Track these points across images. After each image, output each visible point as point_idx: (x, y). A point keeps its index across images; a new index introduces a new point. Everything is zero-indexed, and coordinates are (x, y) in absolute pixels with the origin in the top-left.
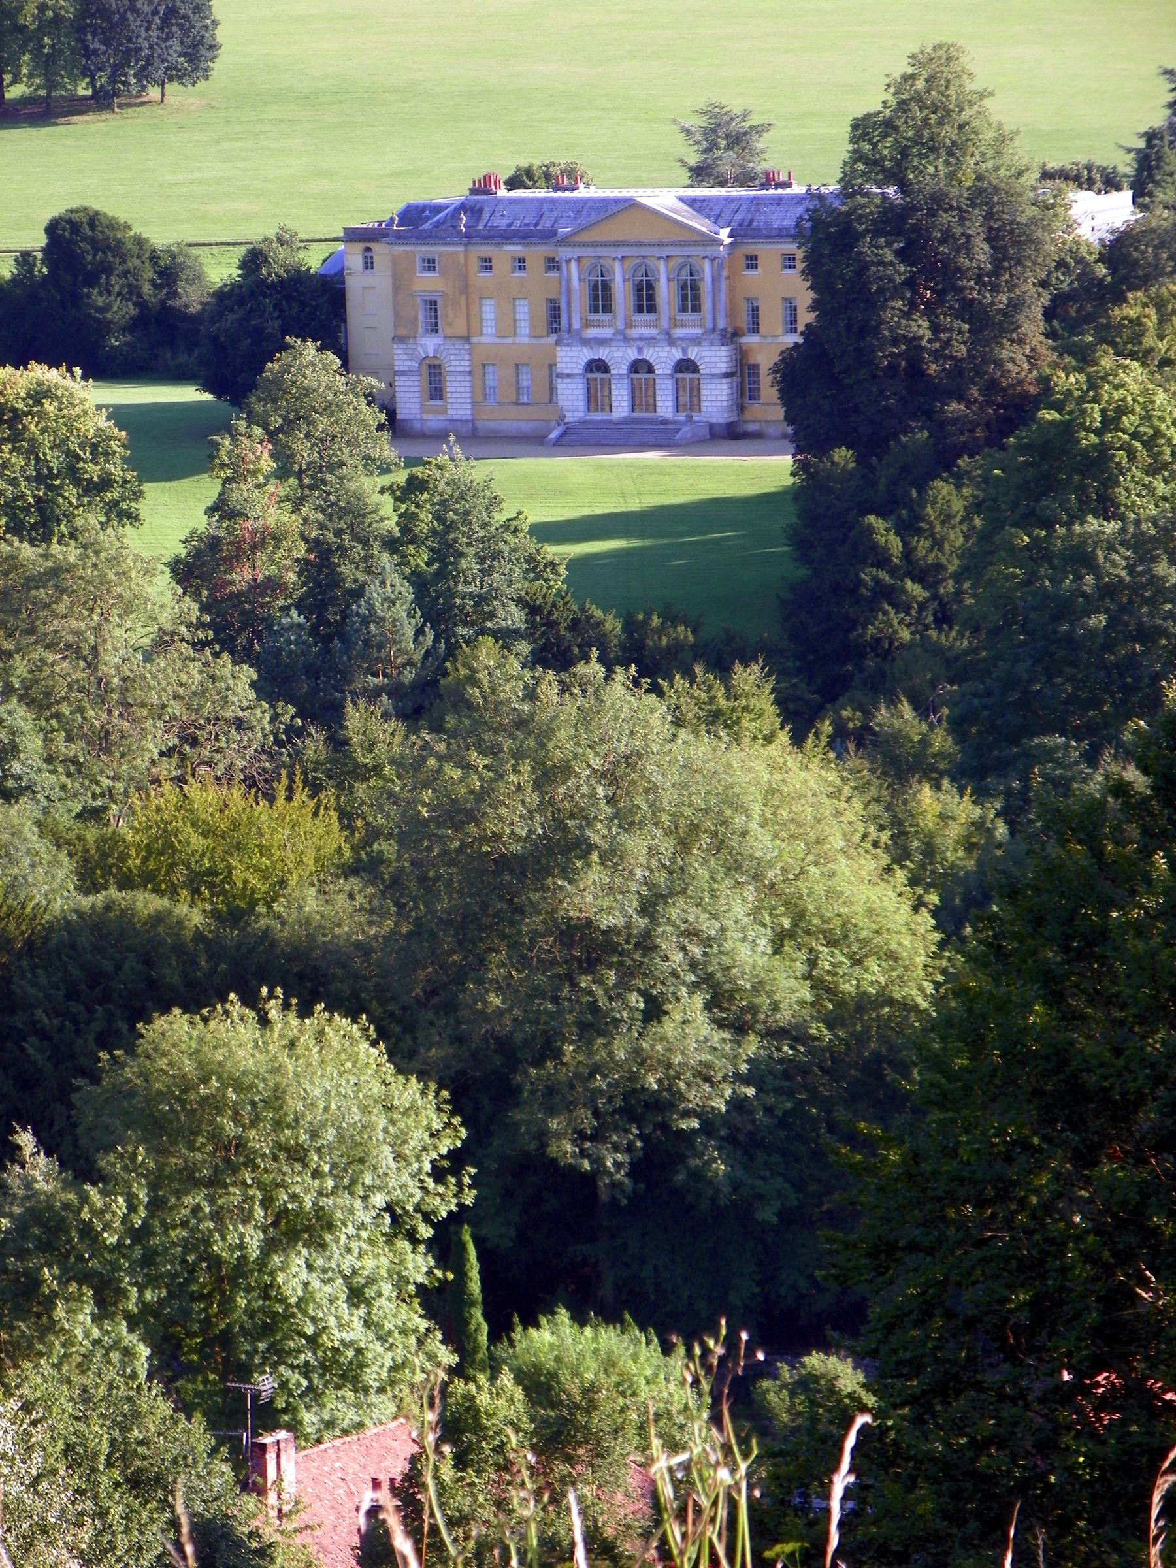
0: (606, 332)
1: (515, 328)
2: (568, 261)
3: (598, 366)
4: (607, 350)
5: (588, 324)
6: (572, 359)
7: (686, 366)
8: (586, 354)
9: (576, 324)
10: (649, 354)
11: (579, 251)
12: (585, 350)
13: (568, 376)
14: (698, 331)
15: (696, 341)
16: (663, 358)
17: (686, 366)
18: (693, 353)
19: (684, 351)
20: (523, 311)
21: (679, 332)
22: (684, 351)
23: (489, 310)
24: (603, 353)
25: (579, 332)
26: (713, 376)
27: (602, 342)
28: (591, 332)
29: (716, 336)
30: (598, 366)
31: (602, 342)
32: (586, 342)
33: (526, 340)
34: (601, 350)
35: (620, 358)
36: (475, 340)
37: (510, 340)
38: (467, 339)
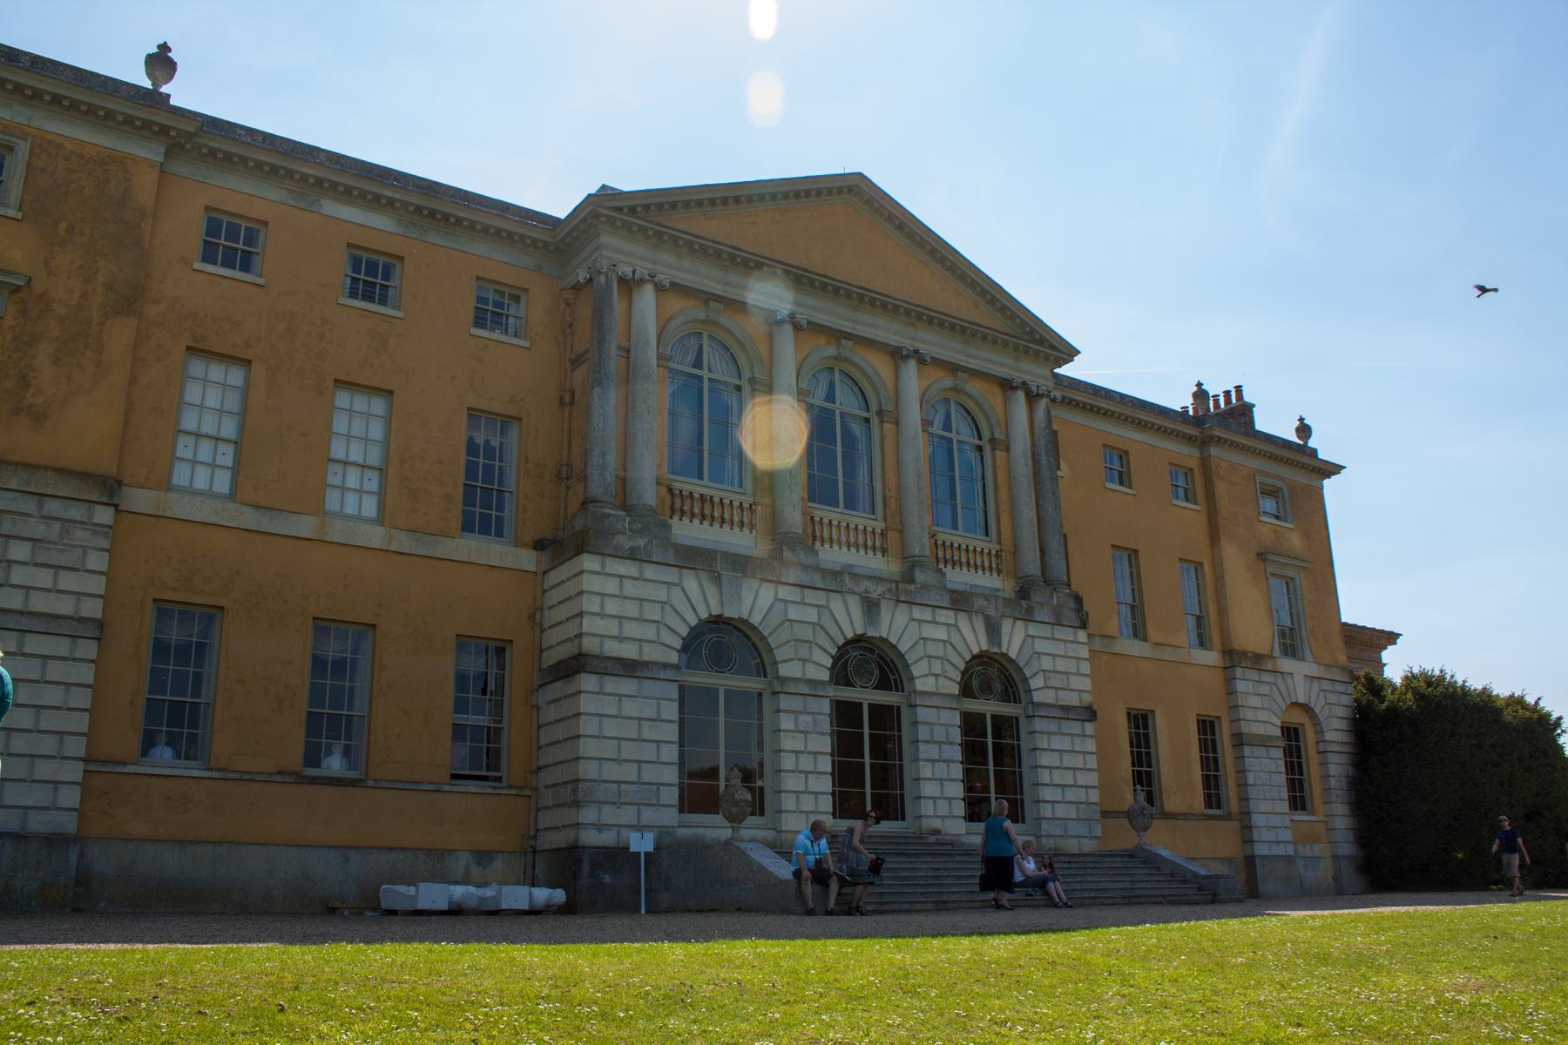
2: (629, 285)
5: (678, 505)
8: (697, 598)
11: (671, 266)
12: (691, 583)
13: (629, 668)
16: (934, 644)
19: (993, 630)
20: (357, 430)
22: (993, 630)
23: (210, 398)
30: (723, 641)
32: (693, 558)
36: (140, 499)
38: (109, 487)
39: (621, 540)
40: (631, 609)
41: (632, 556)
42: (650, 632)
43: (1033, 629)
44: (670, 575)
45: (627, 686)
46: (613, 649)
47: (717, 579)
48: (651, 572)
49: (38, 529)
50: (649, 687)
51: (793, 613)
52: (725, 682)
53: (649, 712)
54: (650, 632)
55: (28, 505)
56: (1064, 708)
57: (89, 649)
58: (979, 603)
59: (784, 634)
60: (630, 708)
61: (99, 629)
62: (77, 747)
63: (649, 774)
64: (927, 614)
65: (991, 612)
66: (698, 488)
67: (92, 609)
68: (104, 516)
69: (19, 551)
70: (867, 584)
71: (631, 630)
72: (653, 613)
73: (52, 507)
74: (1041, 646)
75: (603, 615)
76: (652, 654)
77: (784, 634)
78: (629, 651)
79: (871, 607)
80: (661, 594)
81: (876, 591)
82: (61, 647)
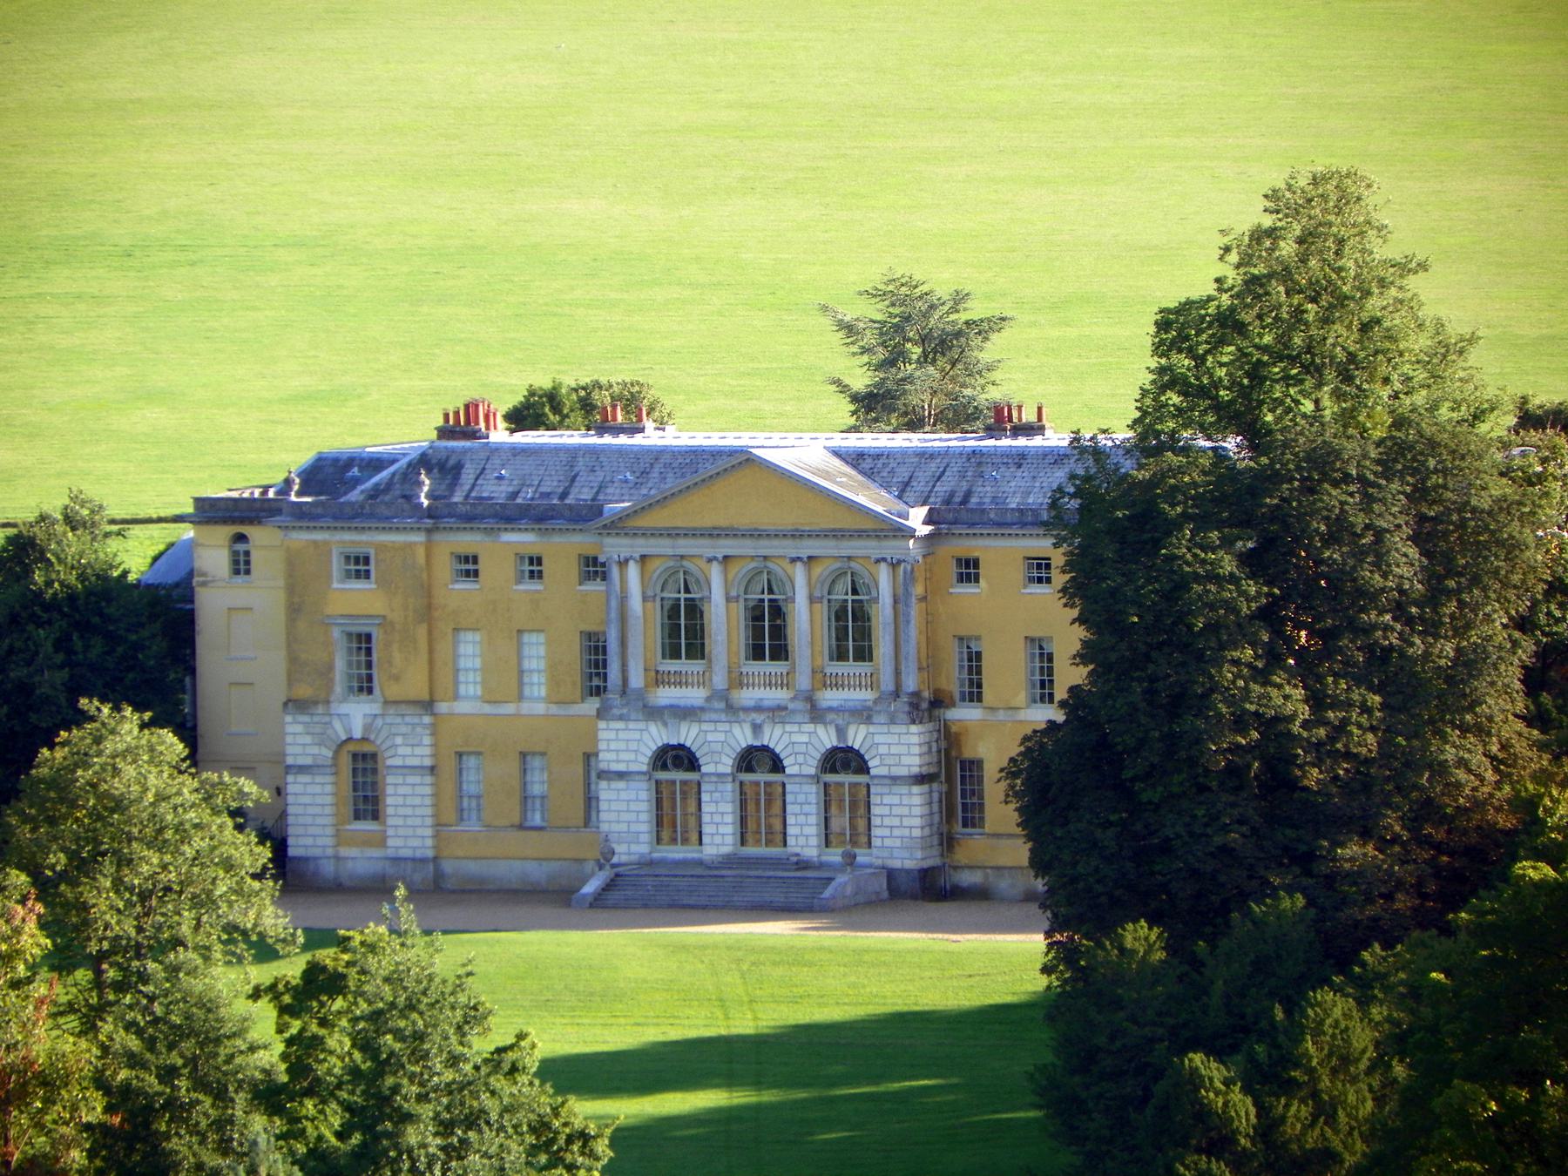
1: (521, 684)
4: (695, 729)
5: (659, 679)
7: (843, 760)
9: (637, 680)
12: (653, 728)
13: (621, 775)
14: (867, 695)
17: (843, 760)
18: (857, 737)
22: (841, 732)
23: (470, 651)
24: (687, 734)
26: (895, 780)
28: (666, 695)
29: (902, 705)
32: (654, 713)
33: (540, 708)
34: (684, 727)
36: (442, 707)
37: (510, 709)
38: (428, 705)
40: (622, 746)
44: (642, 725)
45: (621, 784)
54: (632, 756)
57: (428, 779)
60: (624, 795)
61: (432, 769)
62: (429, 821)
67: (428, 762)
68: (427, 719)
69: (399, 740)
72: (633, 746)
80: (637, 735)
82: (417, 779)
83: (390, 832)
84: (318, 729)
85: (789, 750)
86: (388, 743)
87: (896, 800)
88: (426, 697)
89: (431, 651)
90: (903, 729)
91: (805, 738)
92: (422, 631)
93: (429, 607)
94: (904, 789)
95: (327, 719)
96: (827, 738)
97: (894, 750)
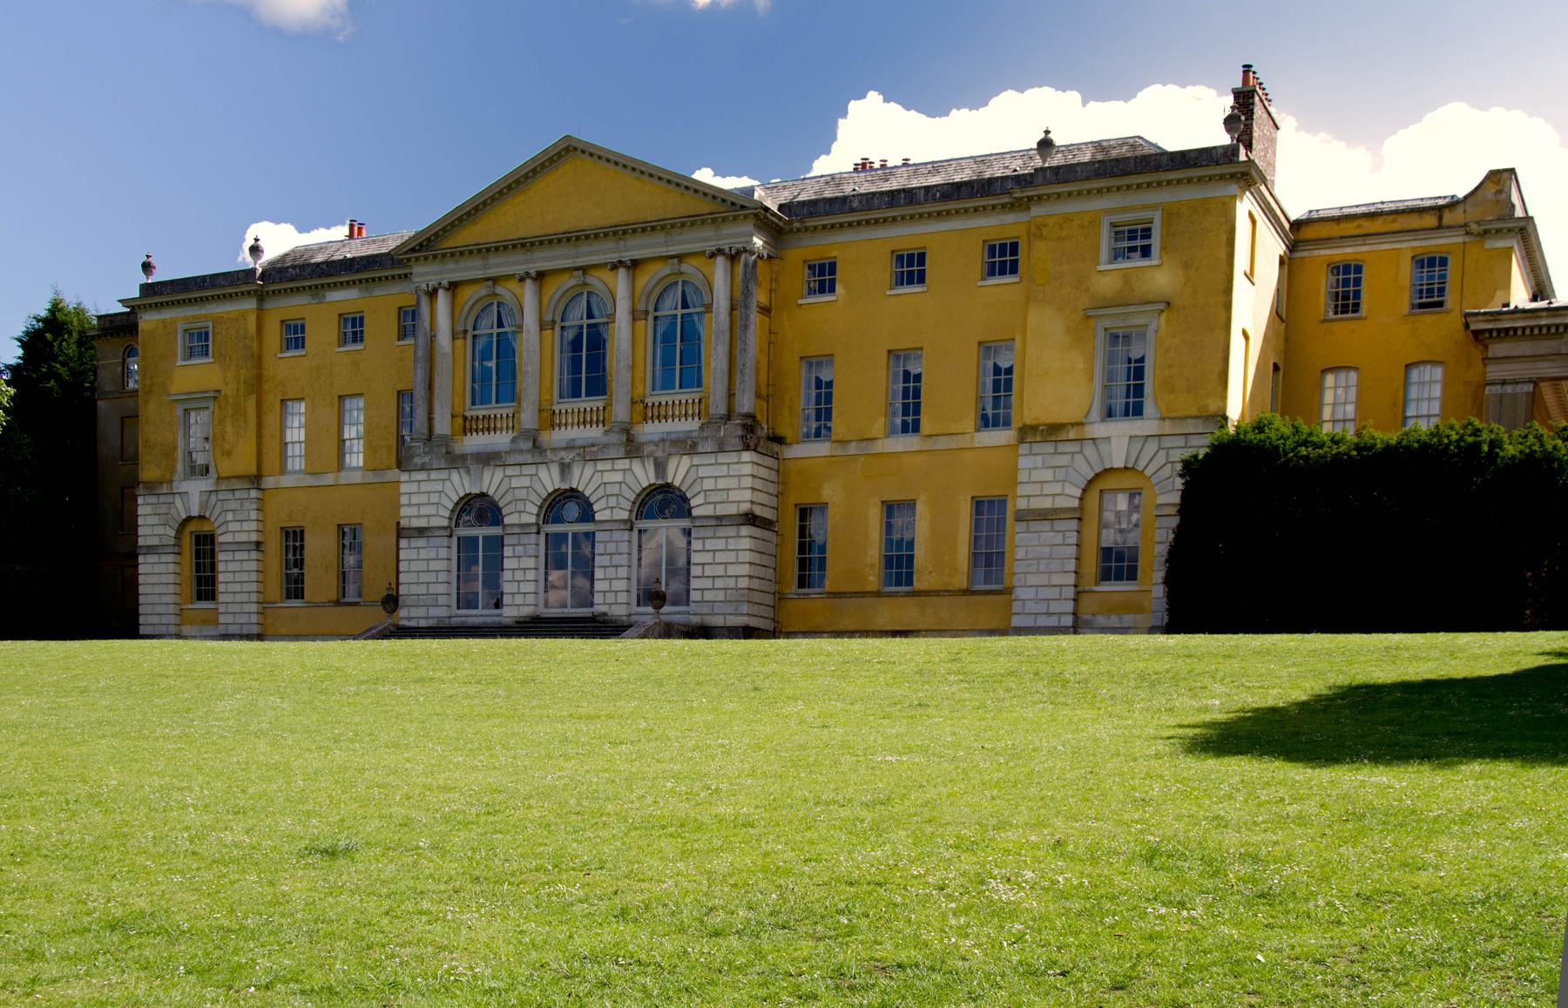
0: (500, 440)
2: (432, 294)
3: (479, 508)
5: (468, 426)
6: (428, 496)
7: (663, 501)
8: (459, 484)
9: (442, 427)
10: (584, 478)
12: (455, 476)
13: (421, 532)
14: (692, 425)
15: (687, 446)
17: (663, 501)
18: (678, 471)
19: (660, 467)
21: (650, 431)
22: (660, 467)
24: (490, 482)
25: (446, 441)
26: (720, 521)
27: (488, 459)
28: (474, 442)
29: (733, 430)
30: (479, 508)
31: (488, 459)
32: (456, 461)
33: (357, 477)
35: (522, 490)
36: (269, 482)
37: (329, 479)
38: (256, 480)
39: (418, 460)
41: (423, 468)
42: (432, 510)
43: (696, 460)
44: (444, 475)
45: (421, 542)
46: (416, 523)
47: (468, 471)
48: (434, 475)
49: (234, 505)
50: (433, 541)
51: (515, 483)
52: (481, 532)
53: (432, 555)
54: (432, 510)
55: (229, 496)
56: (718, 518)
58: (648, 449)
59: (509, 497)
60: (424, 554)
61: (258, 544)
63: (434, 589)
64: (608, 465)
65: (659, 454)
66: (480, 411)
67: (254, 537)
68: (254, 493)
69: (230, 516)
70: (563, 454)
71: (425, 510)
72: (434, 498)
73: (238, 494)
74: (703, 472)
75: (410, 505)
76: (435, 522)
77: (509, 497)
78: (422, 523)
79: (565, 468)
81: (568, 457)
82: (244, 555)
83: (222, 609)
84: (163, 509)
85: (601, 492)
86: (221, 520)
87: (720, 544)
88: (254, 471)
89: (260, 425)
90: (733, 457)
91: (618, 477)
92: (251, 403)
93: (259, 378)
94: (732, 531)
95: (169, 499)
96: (643, 475)
97: (722, 484)
